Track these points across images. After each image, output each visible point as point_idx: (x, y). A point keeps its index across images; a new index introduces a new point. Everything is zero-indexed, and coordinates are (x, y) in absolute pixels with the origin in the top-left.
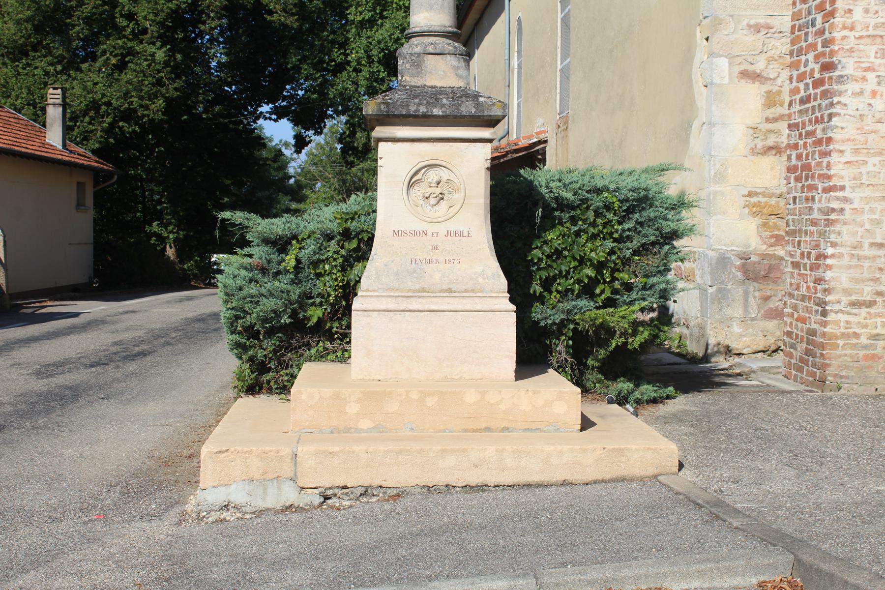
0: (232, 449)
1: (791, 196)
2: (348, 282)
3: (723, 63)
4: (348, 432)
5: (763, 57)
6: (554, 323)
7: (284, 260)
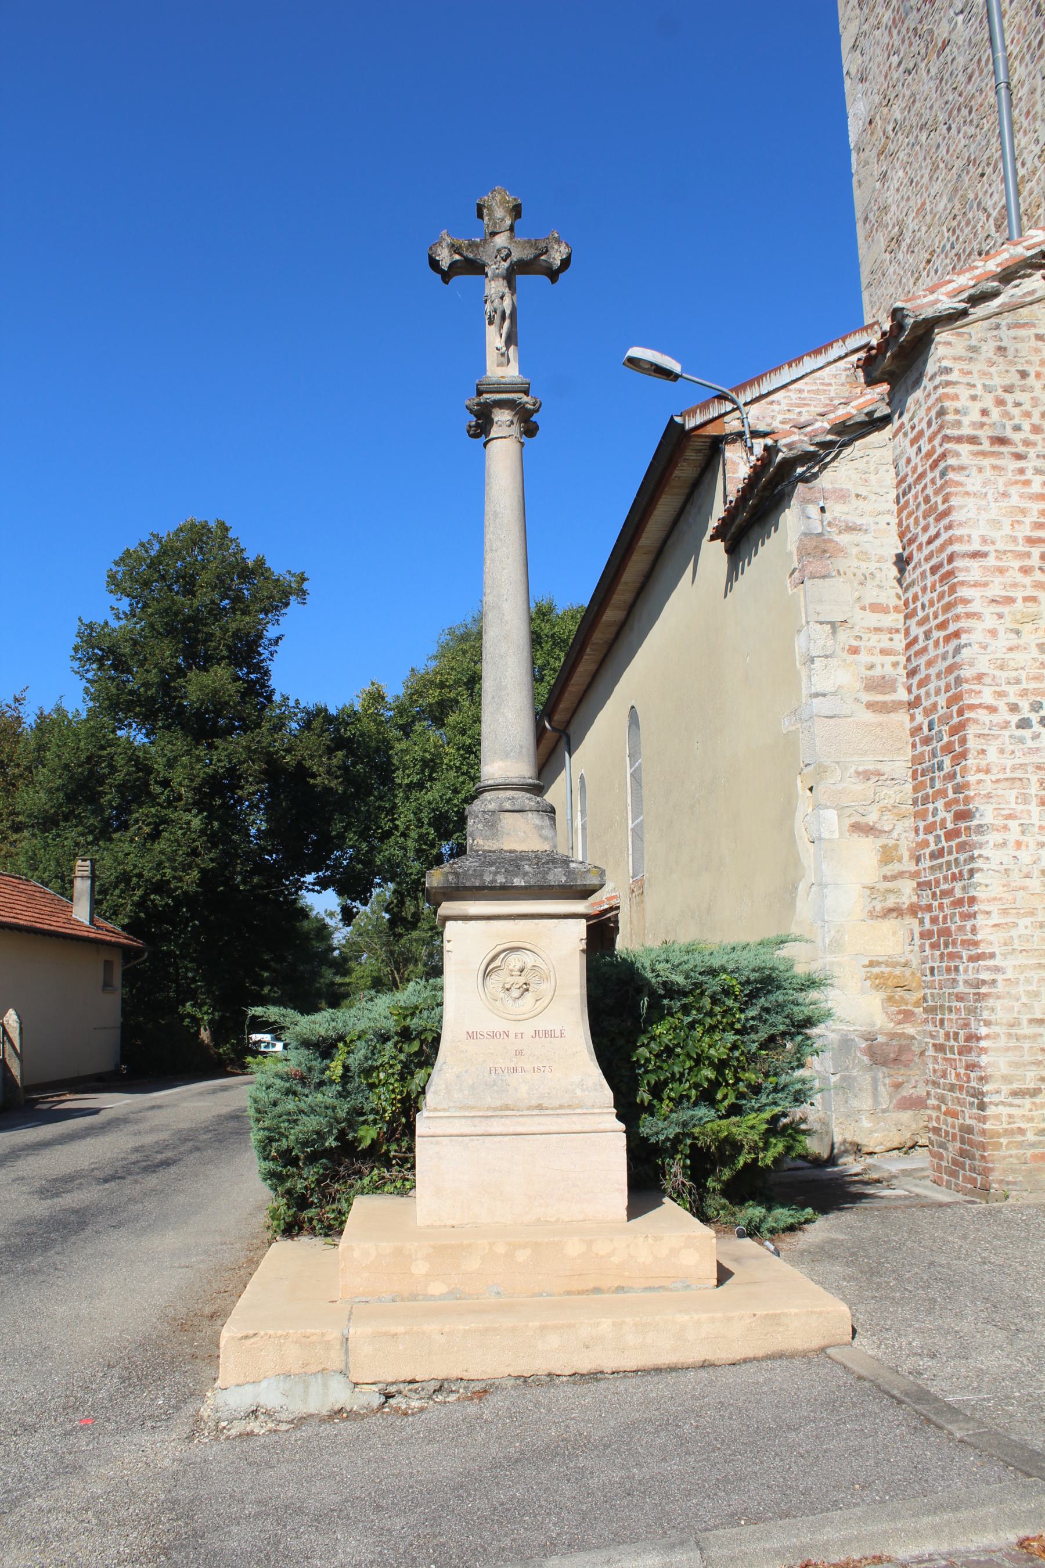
0: (262, 1333)
1: (928, 966)
2: (409, 1094)
3: (831, 815)
4: (415, 1300)
5: (875, 808)
6: (667, 1139)
7: (328, 1068)
